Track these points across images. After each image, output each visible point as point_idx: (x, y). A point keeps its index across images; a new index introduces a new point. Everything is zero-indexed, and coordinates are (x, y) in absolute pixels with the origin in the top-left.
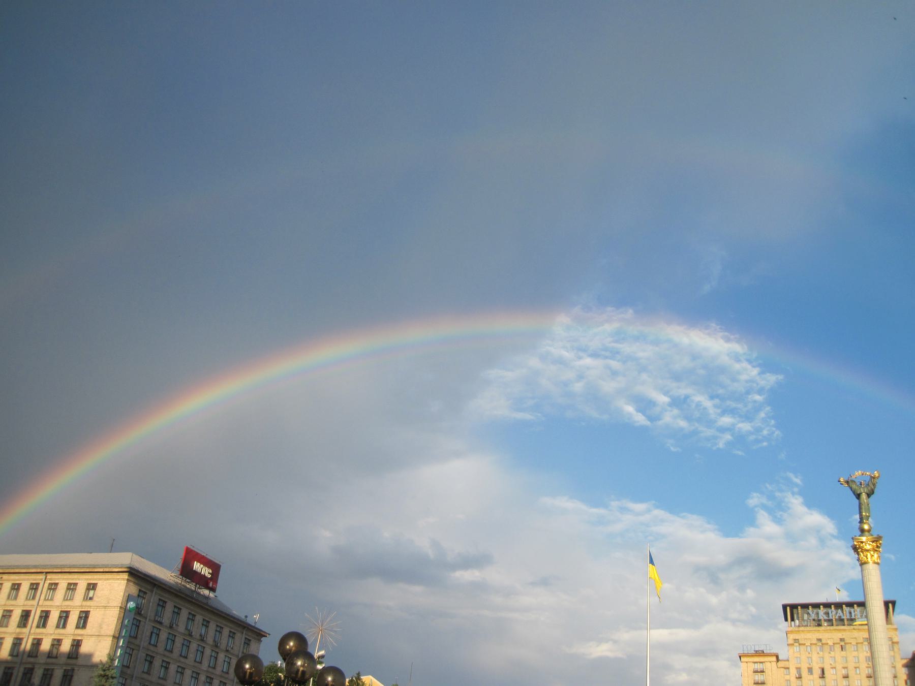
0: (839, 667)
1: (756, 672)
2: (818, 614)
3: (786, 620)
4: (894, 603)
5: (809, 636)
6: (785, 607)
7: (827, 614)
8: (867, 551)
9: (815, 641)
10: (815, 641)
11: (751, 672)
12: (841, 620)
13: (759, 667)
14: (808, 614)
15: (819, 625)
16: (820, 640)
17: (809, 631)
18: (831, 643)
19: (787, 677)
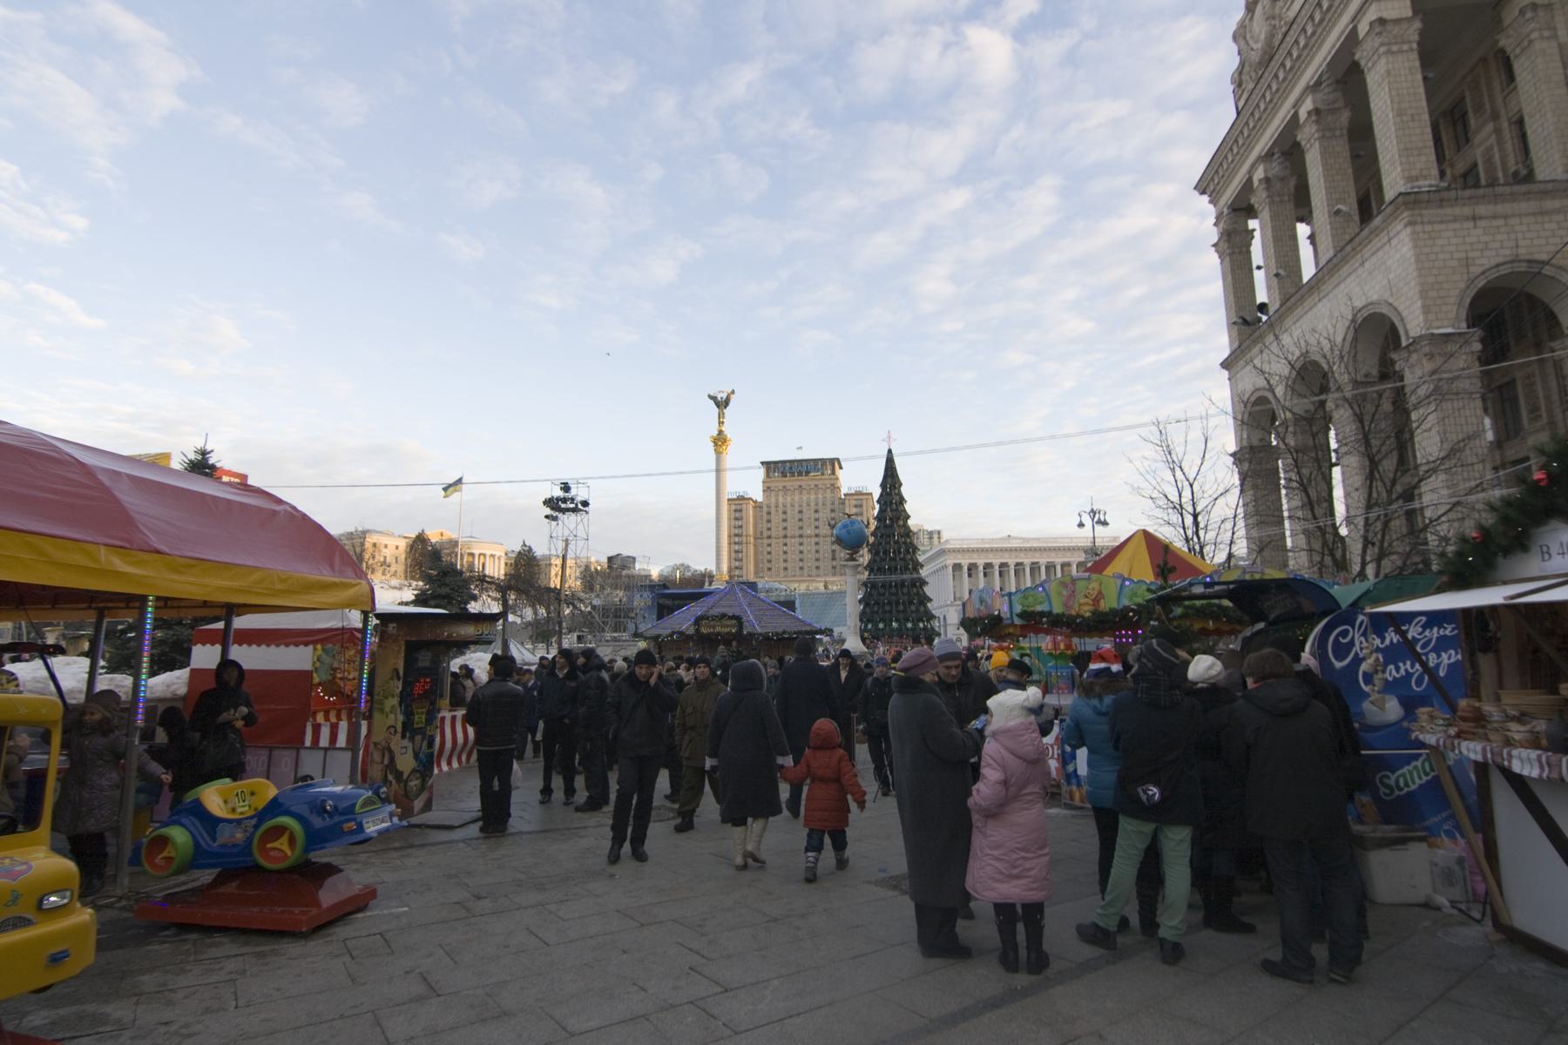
12: (800, 474)
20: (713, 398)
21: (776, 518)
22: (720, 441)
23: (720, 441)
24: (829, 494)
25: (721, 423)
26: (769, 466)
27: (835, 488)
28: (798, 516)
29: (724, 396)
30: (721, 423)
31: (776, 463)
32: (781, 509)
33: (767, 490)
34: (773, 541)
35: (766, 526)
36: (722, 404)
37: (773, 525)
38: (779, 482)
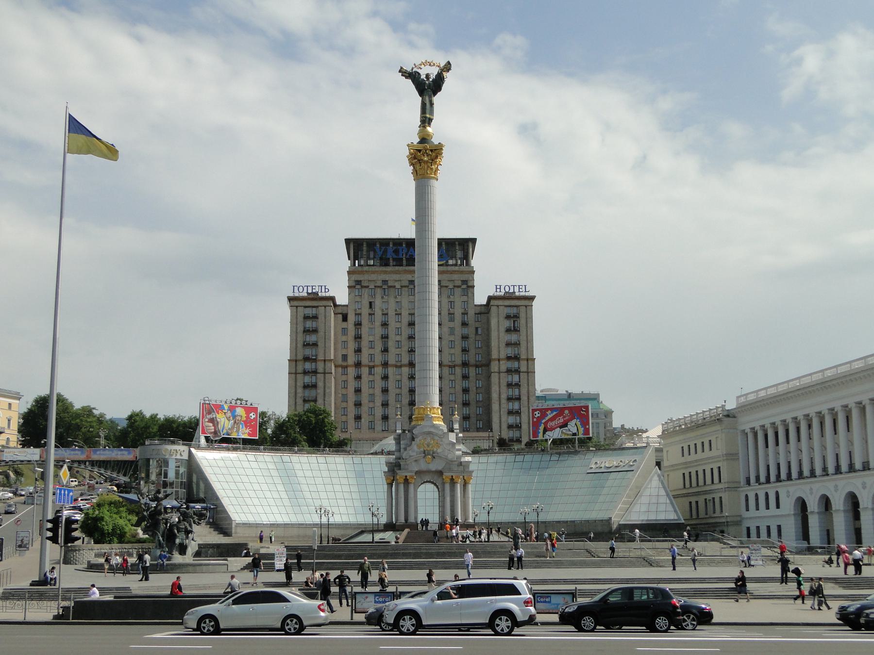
0: (405, 313)
1: (306, 318)
2: (385, 252)
3: (349, 259)
4: (474, 241)
5: (373, 277)
6: (348, 241)
7: (396, 252)
8: (427, 162)
9: (379, 283)
10: (379, 283)
11: (300, 319)
13: (309, 312)
14: (375, 251)
15: (387, 265)
16: (385, 282)
17: (373, 272)
18: (398, 286)
19: (344, 325)
20: (413, 76)
21: (371, 333)
22: (425, 157)
23: (425, 157)
24: (458, 299)
25: (426, 121)
26: (358, 248)
27: (468, 287)
28: (406, 331)
29: (434, 72)
30: (426, 121)
31: (371, 243)
32: (379, 318)
33: (355, 286)
34: (365, 371)
35: (352, 345)
36: (429, 88)
37: (365, 344)
38: (377, 275)
